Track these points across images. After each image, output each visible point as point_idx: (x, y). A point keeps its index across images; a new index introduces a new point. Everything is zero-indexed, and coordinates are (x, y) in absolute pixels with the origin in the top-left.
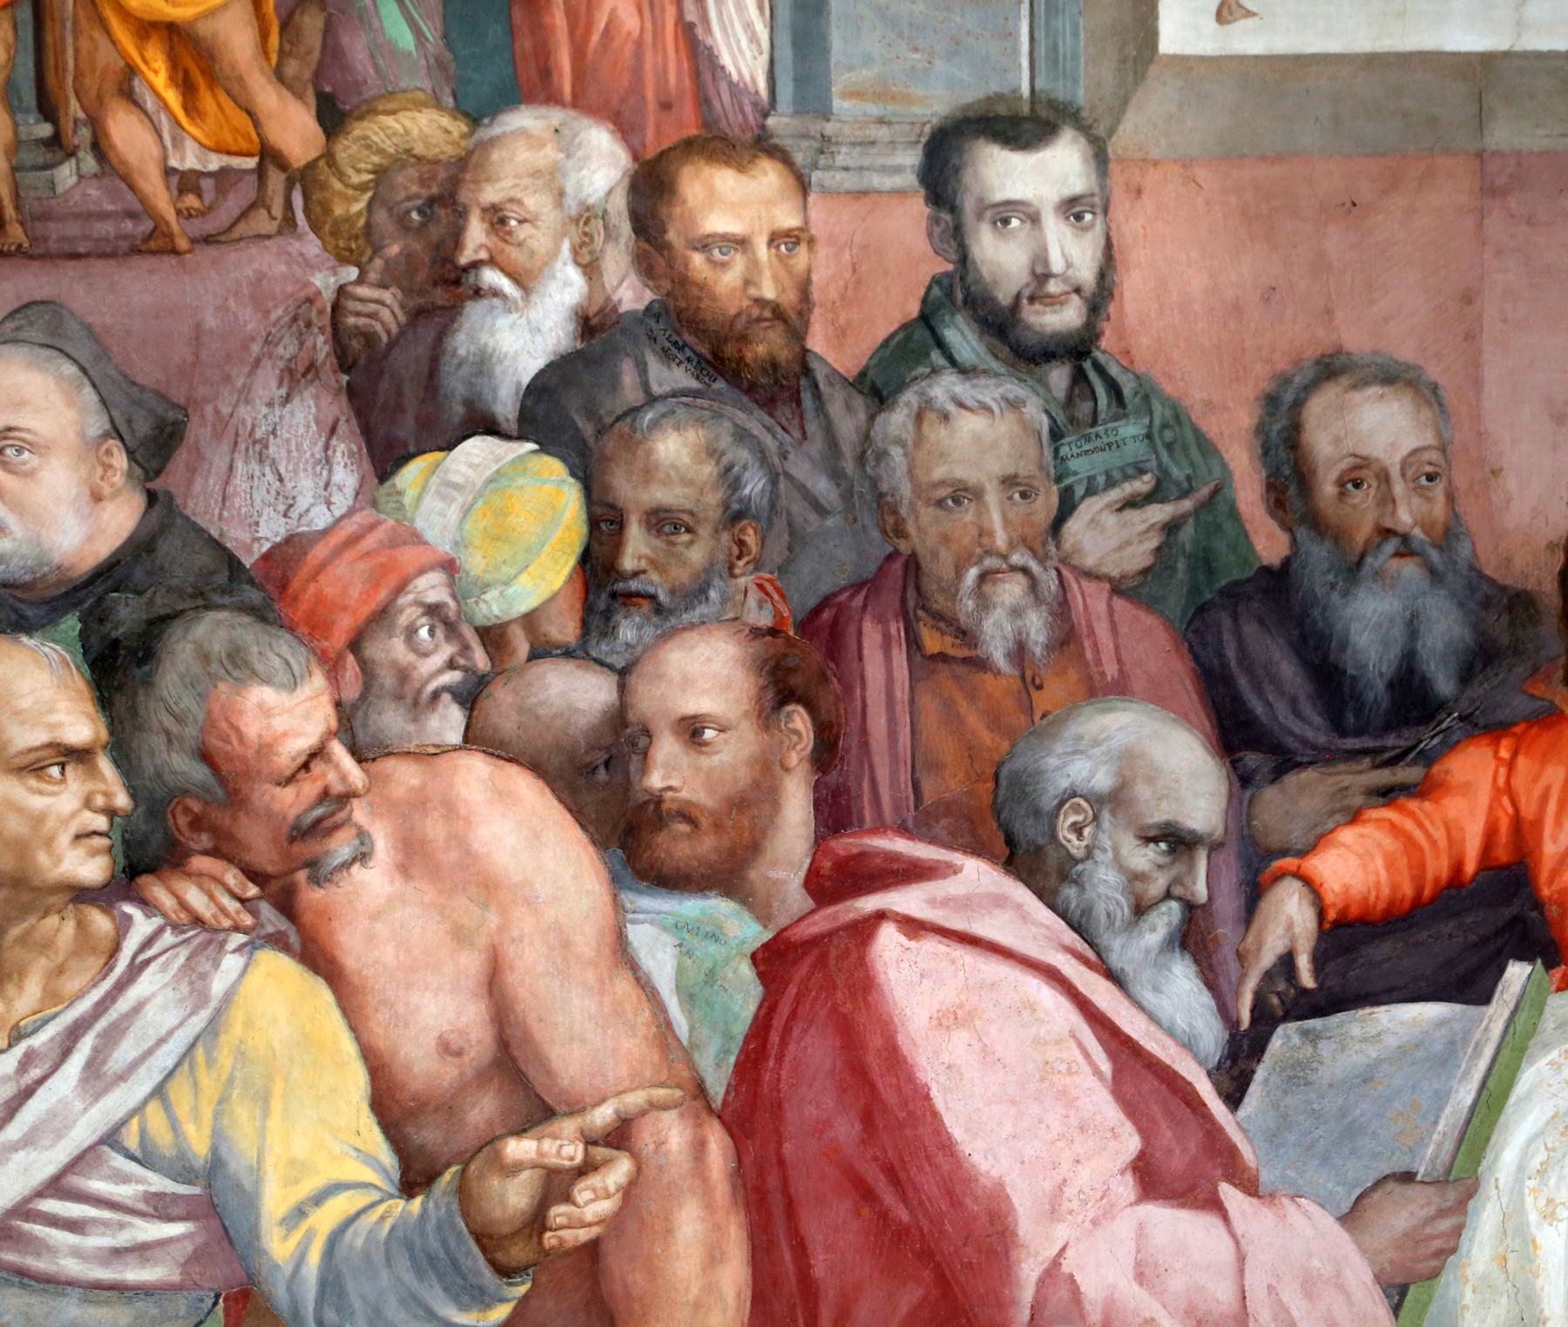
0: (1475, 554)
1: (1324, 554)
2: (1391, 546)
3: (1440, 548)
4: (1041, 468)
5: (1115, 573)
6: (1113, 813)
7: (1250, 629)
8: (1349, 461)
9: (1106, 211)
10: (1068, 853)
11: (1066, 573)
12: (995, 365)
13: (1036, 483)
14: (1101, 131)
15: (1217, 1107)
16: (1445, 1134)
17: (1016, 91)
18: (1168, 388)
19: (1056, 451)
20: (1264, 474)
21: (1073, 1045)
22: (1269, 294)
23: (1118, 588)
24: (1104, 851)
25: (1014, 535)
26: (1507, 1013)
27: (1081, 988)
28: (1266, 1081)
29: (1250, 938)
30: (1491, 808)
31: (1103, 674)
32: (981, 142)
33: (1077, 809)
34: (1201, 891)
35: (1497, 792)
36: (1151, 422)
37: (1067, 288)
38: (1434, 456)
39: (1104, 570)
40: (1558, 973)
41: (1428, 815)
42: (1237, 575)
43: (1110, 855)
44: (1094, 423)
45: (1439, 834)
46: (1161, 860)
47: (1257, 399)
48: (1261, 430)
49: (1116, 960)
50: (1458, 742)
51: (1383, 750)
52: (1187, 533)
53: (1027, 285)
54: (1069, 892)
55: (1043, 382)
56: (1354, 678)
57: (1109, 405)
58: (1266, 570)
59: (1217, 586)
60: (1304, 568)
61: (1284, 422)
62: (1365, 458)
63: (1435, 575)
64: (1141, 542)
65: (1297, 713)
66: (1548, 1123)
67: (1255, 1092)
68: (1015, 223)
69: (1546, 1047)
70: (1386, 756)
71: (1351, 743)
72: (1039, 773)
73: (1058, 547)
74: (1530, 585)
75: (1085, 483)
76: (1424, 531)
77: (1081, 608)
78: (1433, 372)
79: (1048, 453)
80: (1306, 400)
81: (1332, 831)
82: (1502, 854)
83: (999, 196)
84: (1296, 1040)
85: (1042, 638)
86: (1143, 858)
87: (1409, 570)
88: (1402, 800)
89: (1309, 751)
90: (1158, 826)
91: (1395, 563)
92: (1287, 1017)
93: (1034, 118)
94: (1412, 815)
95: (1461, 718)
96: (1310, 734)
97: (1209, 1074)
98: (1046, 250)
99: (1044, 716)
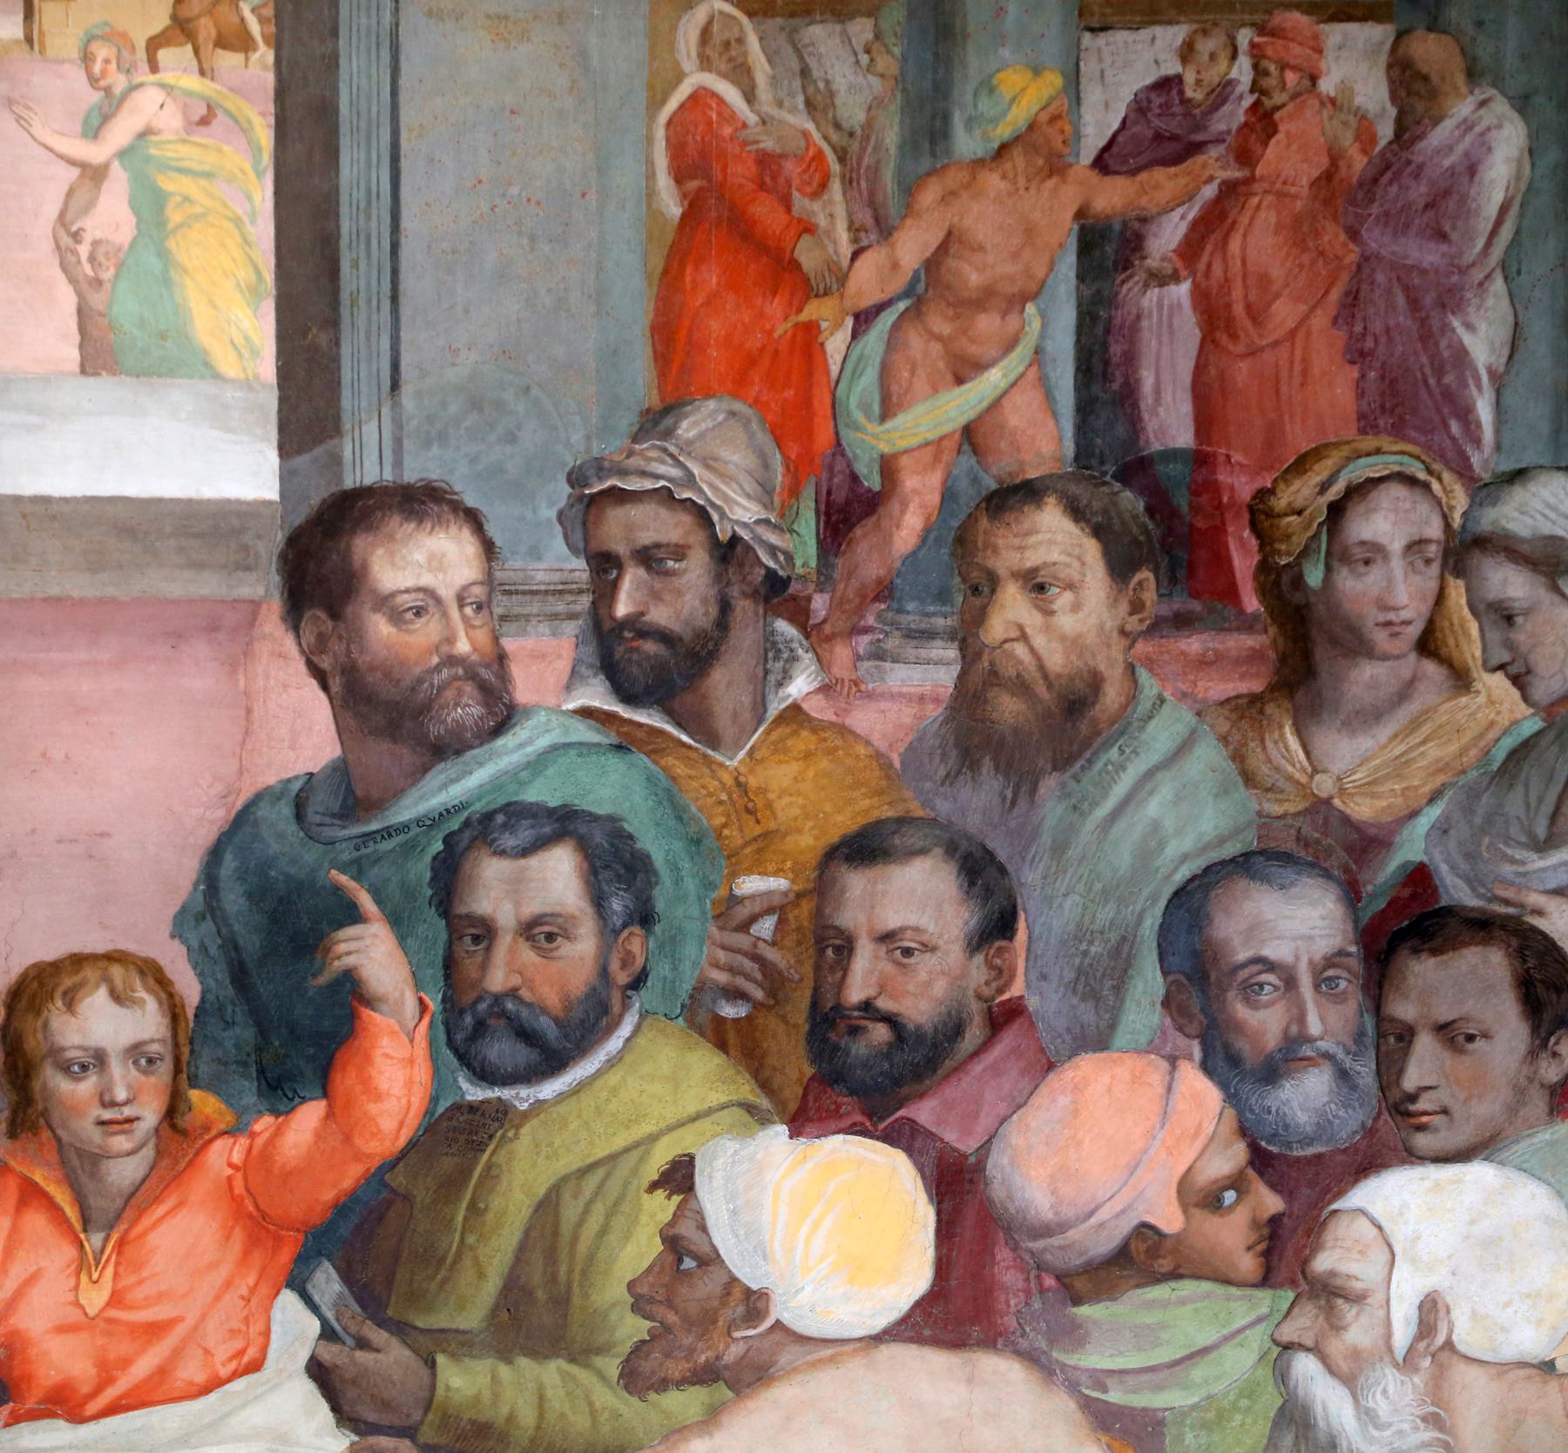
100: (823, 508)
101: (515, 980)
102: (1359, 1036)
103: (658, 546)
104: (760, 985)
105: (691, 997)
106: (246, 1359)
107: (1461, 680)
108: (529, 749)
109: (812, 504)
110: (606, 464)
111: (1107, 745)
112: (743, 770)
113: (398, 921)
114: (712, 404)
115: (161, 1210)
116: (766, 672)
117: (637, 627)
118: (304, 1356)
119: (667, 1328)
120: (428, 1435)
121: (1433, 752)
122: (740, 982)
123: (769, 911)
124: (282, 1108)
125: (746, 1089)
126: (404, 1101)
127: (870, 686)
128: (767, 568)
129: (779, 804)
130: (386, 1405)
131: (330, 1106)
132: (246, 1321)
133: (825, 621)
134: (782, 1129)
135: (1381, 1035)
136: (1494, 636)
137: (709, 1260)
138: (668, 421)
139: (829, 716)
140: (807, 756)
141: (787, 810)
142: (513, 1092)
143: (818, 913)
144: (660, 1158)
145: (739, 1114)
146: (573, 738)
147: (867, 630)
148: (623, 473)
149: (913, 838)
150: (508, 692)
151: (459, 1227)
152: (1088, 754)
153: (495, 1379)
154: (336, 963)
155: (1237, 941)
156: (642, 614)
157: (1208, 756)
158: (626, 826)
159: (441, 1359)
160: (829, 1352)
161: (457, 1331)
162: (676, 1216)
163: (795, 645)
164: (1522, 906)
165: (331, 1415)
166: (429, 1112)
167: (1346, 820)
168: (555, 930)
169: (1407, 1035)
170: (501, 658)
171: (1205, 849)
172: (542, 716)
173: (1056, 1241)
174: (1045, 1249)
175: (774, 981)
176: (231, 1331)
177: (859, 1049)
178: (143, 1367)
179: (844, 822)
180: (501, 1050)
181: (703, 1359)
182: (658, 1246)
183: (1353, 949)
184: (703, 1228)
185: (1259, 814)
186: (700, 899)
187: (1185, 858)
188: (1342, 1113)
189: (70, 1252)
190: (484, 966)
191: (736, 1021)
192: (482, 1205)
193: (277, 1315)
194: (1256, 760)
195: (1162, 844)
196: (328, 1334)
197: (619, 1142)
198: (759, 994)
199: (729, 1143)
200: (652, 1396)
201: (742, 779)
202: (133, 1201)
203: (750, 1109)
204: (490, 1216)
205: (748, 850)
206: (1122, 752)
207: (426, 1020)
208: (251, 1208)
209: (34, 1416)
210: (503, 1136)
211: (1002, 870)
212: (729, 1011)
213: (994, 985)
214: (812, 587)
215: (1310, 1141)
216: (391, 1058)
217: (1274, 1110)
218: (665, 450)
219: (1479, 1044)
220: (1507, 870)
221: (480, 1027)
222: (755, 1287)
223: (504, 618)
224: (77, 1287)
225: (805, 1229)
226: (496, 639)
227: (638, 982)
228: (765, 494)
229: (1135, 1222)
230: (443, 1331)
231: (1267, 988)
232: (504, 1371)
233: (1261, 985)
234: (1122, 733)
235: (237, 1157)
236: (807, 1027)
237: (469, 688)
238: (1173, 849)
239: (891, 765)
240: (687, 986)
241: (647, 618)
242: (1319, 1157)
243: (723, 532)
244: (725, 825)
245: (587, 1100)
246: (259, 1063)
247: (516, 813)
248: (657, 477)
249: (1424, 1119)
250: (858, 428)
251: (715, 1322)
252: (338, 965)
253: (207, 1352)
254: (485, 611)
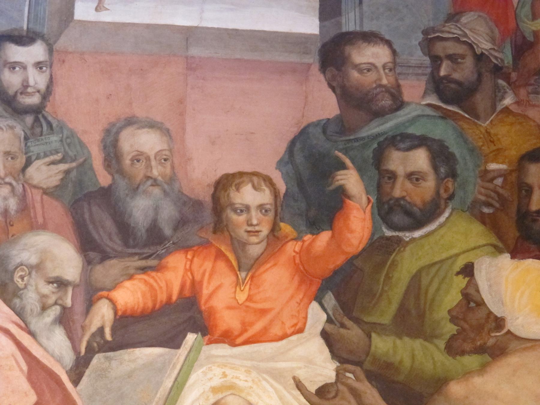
0: (181, 187)
1: (124, 184)
2: (149, 182)
3: (168, 184)
4: (20, 149)
5: (45, 187)
6: (36, 272)
7: (95, 209)
8: (136, 153)
9: (51, 67)
10: (17, 286)
11: (26, 186)
12: (5, 114)
13: (17, 154)
14: (51, 42)
15: (69, 385)
16: (159, 398)
17: (22, 27)
18: (70, 126)
19: (26, 144)
20: (103, 155)
21: (12, 359)
22: (109, 97)
23: (45, 192)
24: (32, 286)
25: (7, 172)
26: (186, 352)
27: (18, 337)
28: (89, 376)
29: (87, 321)
30: (183, 276)
31: (37, 222)
32: (8, 42)
33: (23, 270)
34: (68, 302)
35: (186, 270)
36: (63, 136)
37: (34, 91)
38: (167, 153)
39: (41, 185)
40: (207, 338)
41: (159, 278)
42: (91, 189)
43: (34, 288)
44: (41, 135)
45: (163, 284)
46: (54, 290)
47: (102, 130)
48: (103, 140)
49: (33, 327)
50: (171, 252)
51: (143, 253)
52: (74, 174)
53: (20, 89)
54: (17, 301)
55: (23, 121)
56: (133, 227)
57: (47, 130)
58: (102, 189)
59: (84, 193)
60: (116, 188)
61: (112, 139)
62: (142, 152)
63: (166, 193)
64: (55, 176)
65: (111, 239)
66: (200, 395)
67: (85, 380)
68: (17, 69)
69: (202, 366)
70: (144, 256)
71: (131, 251)
72: (8, 257)
73: (24, 176)
74: (201, 198)
75: (36, 155)
76: (162, 177)
77: (31, 198)
78: (168, 125)
79: (23, 145)
80: (121, 131)
81: (122, 282)
82: (187, 293)
83: (12, 60)
84: (103, 360)
85: (15, 208)
86: (47, 289)
87: (156, 191)
88: (149, 272)
89: (114, 253)
90: (54, 278)
91: (151, 188)
92: (99, 352)
93: (27, 36)
94: (153, 277)
95: (173, 243)
96: (116, 247)
97: (67, 372)
98: (28, 78)
99: (13, 236)
100: (513, 46)
101: (404, 194)
103: (455, 54)
104: (497, 201)
105: (471, 204)
106: (297, 327)
108: (409, 116)
109: (510, 45)
110: (436, 29)
112: (488, 127)
113: (361, 171)
114: (472, 13)
115: (268, 265)
116: (496, 96)
117: (447, 78)
118: (320, 328)
119: (464, 330)
120: (367, 365)
122: (490, 200)
123: (500, 176)
124: (315, 233)
125: (494, 240)
126: (361, 234)
127: (534, 103)
128: (495, 64)
130: (351, 352)
131: (333, 233)
132: (298, 312)
133: (516, 81)
134: (508, 255)
137: (481, 304)
138: (457, 17)
139: (520, 112)
140: (512, 124)
142: (403, 234)
144: (460, 263)
145: (491, 249)
146: (426, 113)
147: (531, 85)
148: (442, 32)
150: (402, 98)
151: (382, 283)
153: (395, 346)
154: (337, 183)
156: (450, 75)
158: (445, 143)
159: (373, 335)
160: (529, 345)
161: (379, 324)
162: (467, 286)
163: (505, 88)
165: (329, 354)
166: (371, 238)
168: (419, 177)
170: (399, 86)
172: (413, 106)
176: (292, 315)
178: (258, 326)
179: (527, 147)
180: (398, 218)
181: (479, 343)
182: (460, 297)
184: (478, 291)
186: (474, 170)
189: (233, 278)
190: (392, 188)
191: (489, 214)
192: (391, 275)
193: (310, 311)
196: (329, 320)
197: (444, 256)
198: (497, 205)
199: (487, 259)
200: (458, 357)
201: (488, 130)
202: (257, 262)
203: (495, 246)
204: (394, 279)
205: (491, 155)
207: (370, 205)
208: (302, 269)
209: (217, 341)
210: (399, 250)
212: (486, 210)
214: (510, 71)
216: (357, 218)
218: (456, 26)
221: (391, 210)
222: (499, 315)
223: (399, 74)
224: (235, 292)
225: (518, 294)
226: (397, 80)
227: (451, 197)
228: (493, 40)
230: (375, 323)
232: (398, 342)
235: (297, 249)
236: (516, 218)
237: (387, 95)
240: (469, 201)
241: (452, 77)
243: (478, 52)
244: (482, 146)
245: (432, 239)
246: (307, 215)
247: (405, 137)
248: (454, 34)
250: (524, 22)
251: (483, 329)
252: (337, 184)
253: (283, 323)
254: (393, 71)
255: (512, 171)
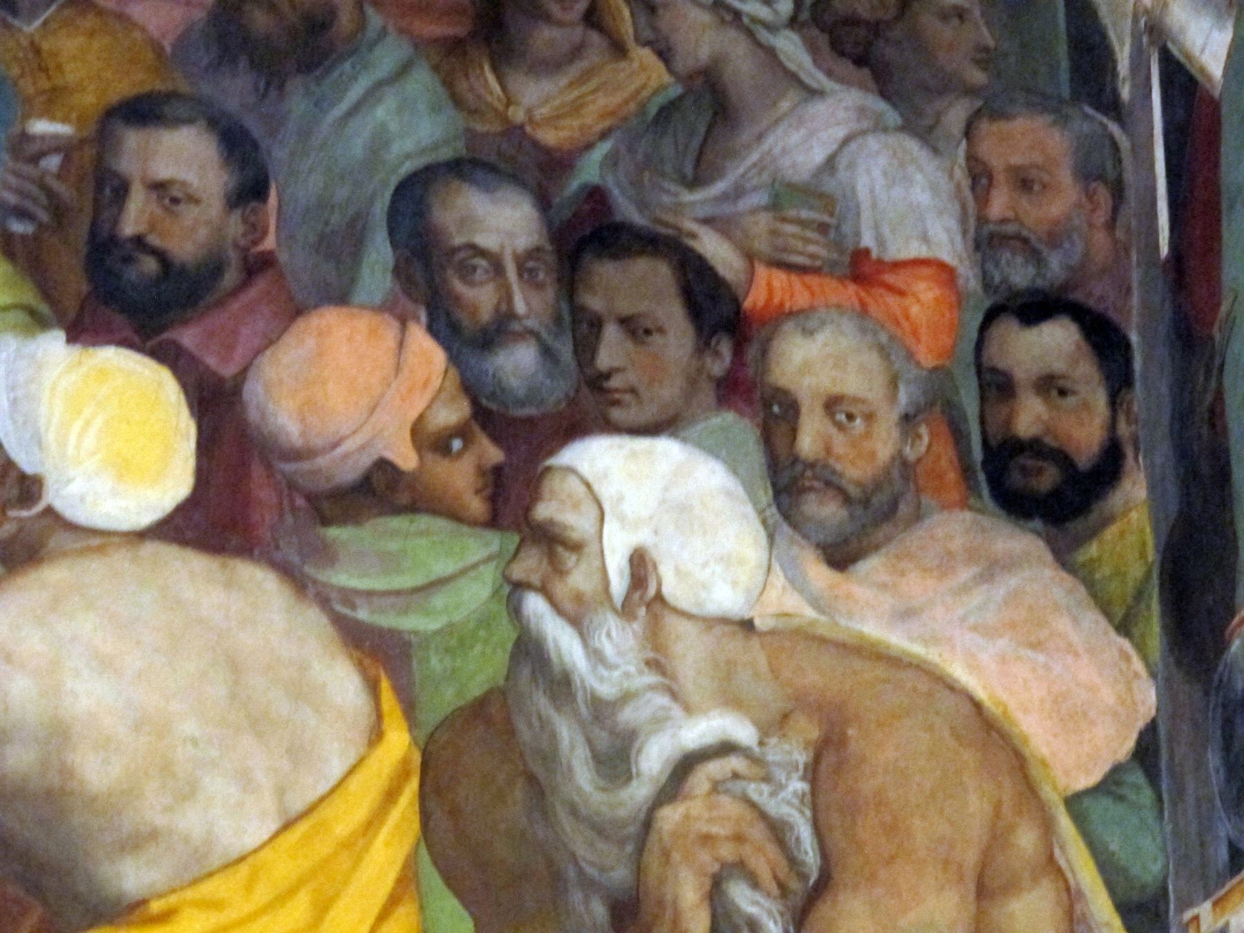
102: (558, 320)
107: (619, 50)
111: (342, 58)
112: (37, 38)
121: (603, 101)
122: (28, 204)
123: (57, 150)
125: (29, 295)
129: (68, 67)
135: (575, 322)
136: (643, 20)
140: (91, 34)
141: (73, 73)
143: (99, 160)
145: (22, 317)
149: (181, 110)
152: (326, 63)
155: (453, 229)
157: (422, 81)
160: (95, 542)
164: (679, 229)
167: (536, 144)
169: (597, 324)
171: (422, 152)
173: (305, 466)
174: (295, 472)
175: (59, 210)
177: (132, 274)
179: (122, 88)
183: (549, 247)
185: (468, 130)
187: (408, 156)
188: (548, 382)
191: (23, 237)
194: (462, 86)
195: (386, 144)
198: (44, 217)
203: (32, 312)
206: (354, 68)
211: (255, 145)
213: (250, 237)
215: (523, 404)
217: (491, 373)
219: (656, 338)
220: (666, 199)
225: (79, 424)
229: (375, 457)
231: (479, 271)
233: (474, 268)
234: (354, 52)
238: (400, 147)
239: (163, 49)
242: (530, 421)
249: (617, 396)
255: (82, 142)
